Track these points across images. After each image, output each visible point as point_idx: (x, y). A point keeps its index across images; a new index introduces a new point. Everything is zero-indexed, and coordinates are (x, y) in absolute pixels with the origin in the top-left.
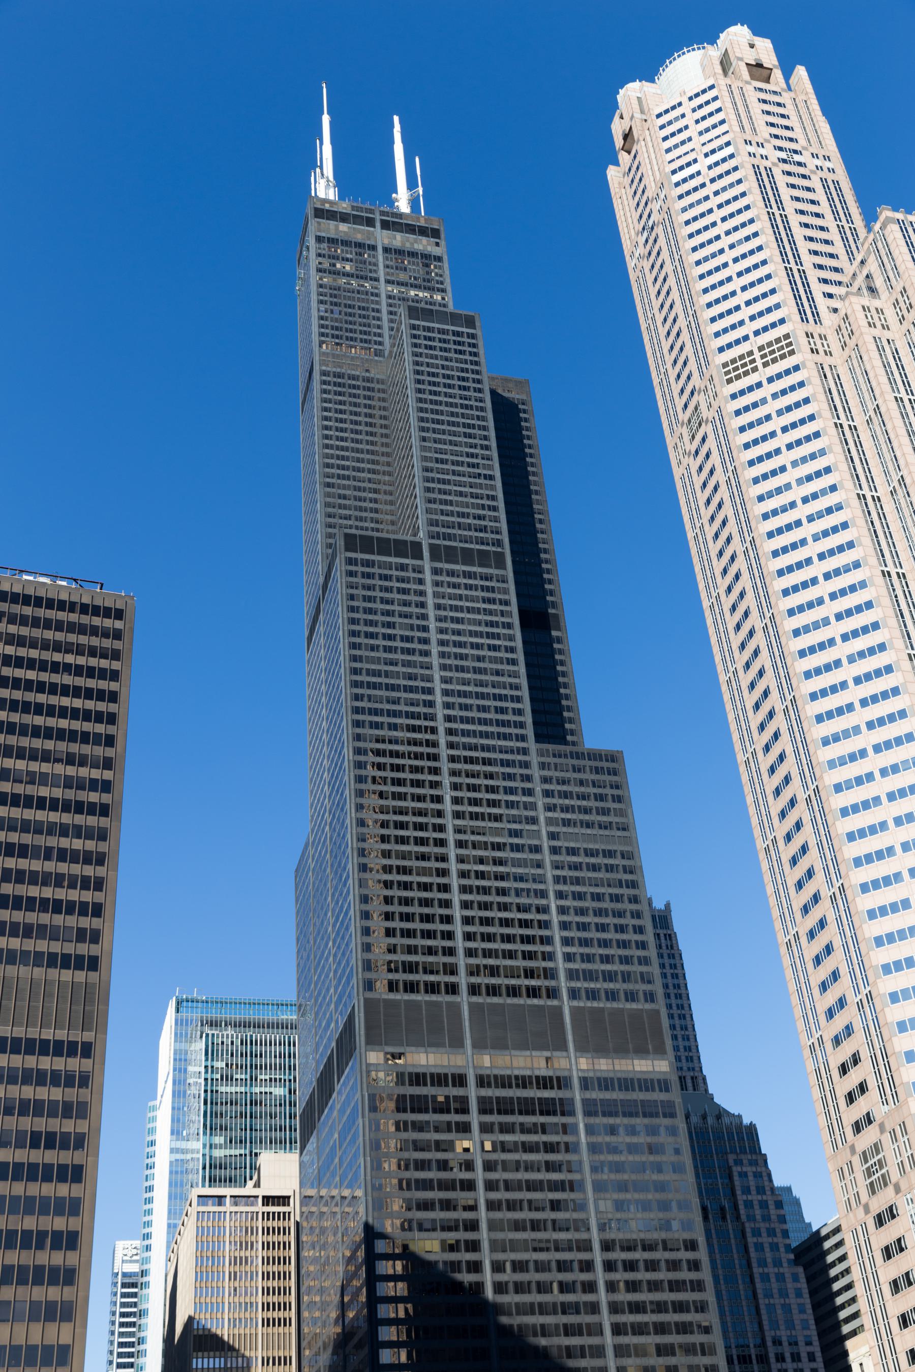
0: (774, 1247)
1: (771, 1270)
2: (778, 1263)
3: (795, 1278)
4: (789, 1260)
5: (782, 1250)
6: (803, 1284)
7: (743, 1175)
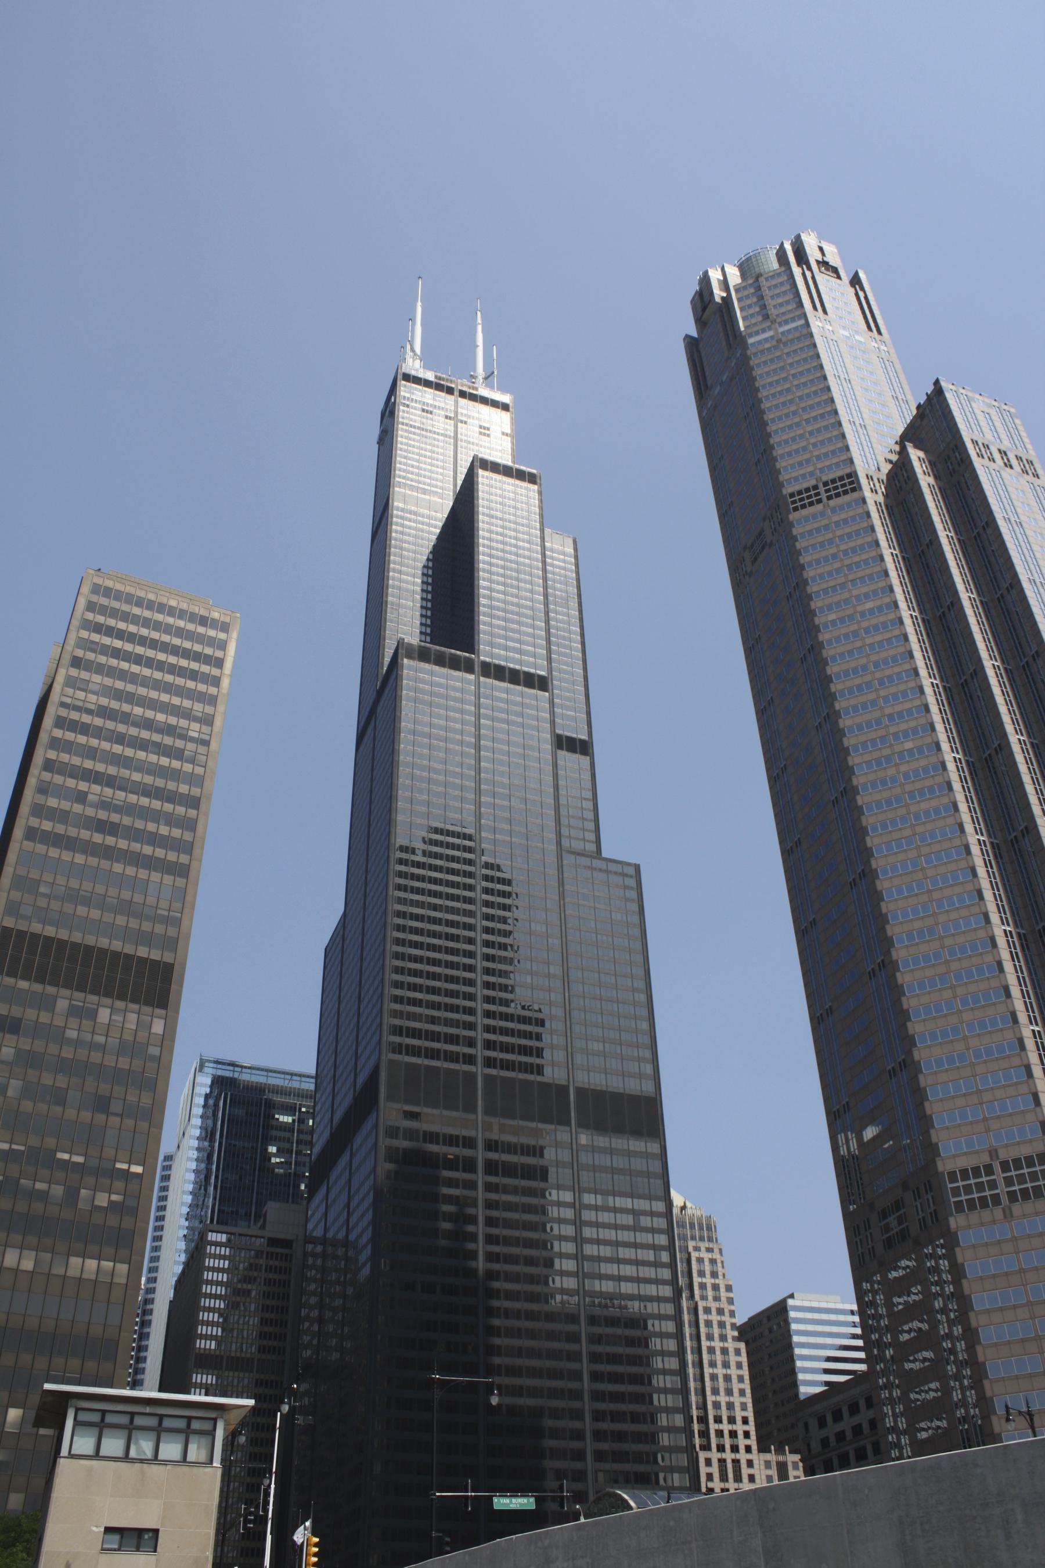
0: (722, 1325)
1: (717, 1344)
2: (723, 1338)
5: (728, 1327)
6: (744, 1359)
7: (700, 1260)
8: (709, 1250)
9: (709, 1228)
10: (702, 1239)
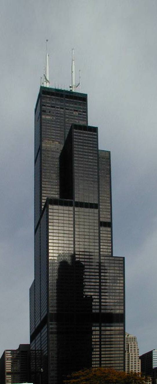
3: (138, 361)
4: (138, 359)
6: (140, 362)
8: (134, 343)
9: (135, 339)
10: (132, 341)
